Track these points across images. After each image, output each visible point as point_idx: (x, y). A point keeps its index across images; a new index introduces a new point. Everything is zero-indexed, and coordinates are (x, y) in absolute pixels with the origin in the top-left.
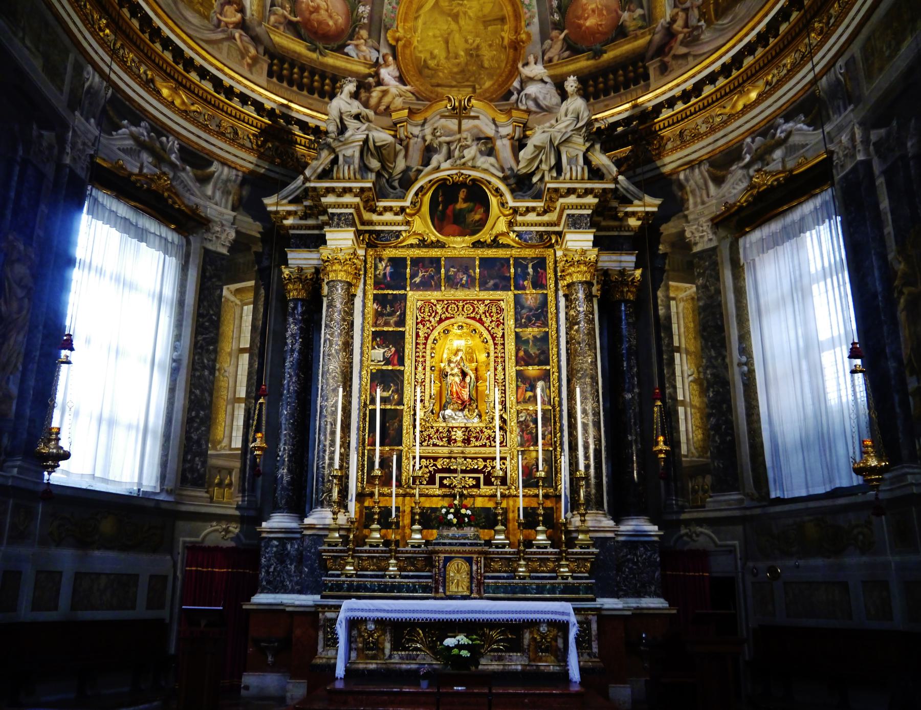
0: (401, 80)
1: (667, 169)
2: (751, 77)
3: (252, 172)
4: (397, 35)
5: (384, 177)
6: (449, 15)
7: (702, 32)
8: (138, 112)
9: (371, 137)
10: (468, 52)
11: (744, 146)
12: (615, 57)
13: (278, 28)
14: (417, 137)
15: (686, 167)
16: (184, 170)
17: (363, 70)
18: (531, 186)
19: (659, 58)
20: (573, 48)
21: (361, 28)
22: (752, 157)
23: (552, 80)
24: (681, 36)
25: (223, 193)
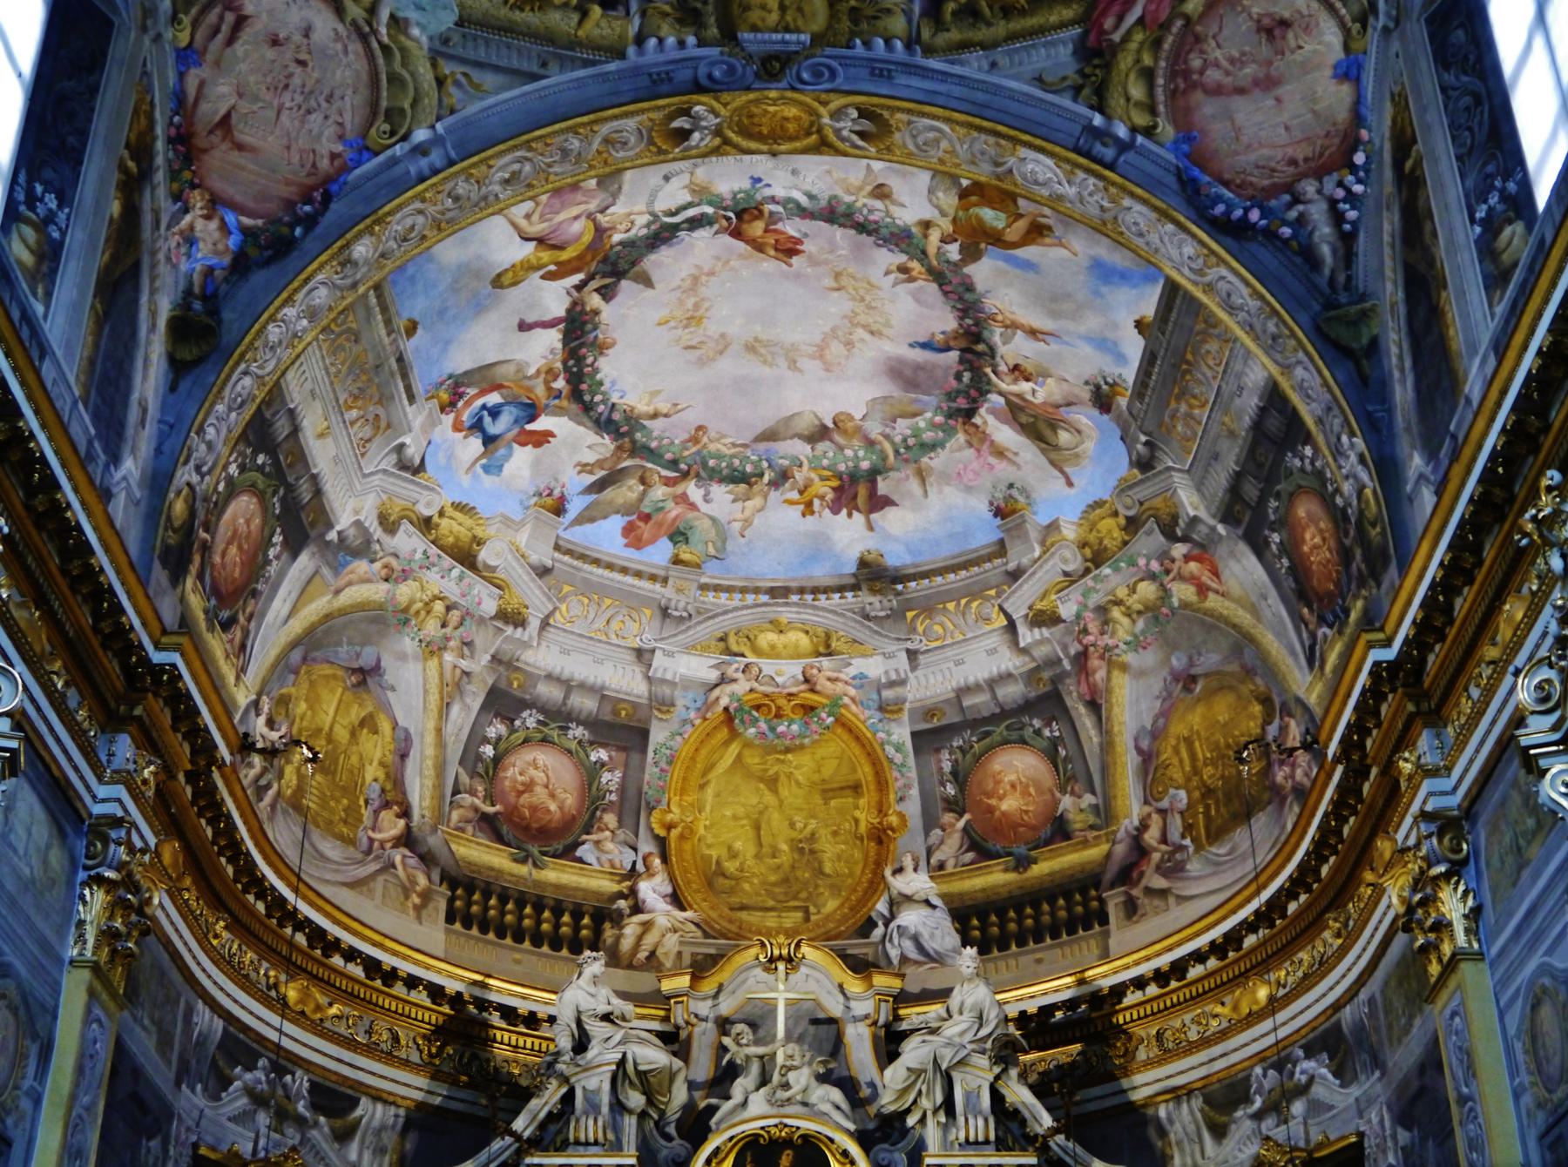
0: (677, 900)
1: (1137, 1096)
2: (1262, 965)
3: (421, 1105)
4: (669, 817)
6: (761, 780)
8: (255, 1045)
9: (630, 1057)
12: (1051, 874)
13: (462, 830)
14: (705, 1020)
15: (1167, 1097)
16: (316, 1124)
17: (608, 886)
18: (905, 1132)
20: (980, 848)
21: (604, 811)
23: (946, 904)
24: (1156, 856)
25: (374, 1152)
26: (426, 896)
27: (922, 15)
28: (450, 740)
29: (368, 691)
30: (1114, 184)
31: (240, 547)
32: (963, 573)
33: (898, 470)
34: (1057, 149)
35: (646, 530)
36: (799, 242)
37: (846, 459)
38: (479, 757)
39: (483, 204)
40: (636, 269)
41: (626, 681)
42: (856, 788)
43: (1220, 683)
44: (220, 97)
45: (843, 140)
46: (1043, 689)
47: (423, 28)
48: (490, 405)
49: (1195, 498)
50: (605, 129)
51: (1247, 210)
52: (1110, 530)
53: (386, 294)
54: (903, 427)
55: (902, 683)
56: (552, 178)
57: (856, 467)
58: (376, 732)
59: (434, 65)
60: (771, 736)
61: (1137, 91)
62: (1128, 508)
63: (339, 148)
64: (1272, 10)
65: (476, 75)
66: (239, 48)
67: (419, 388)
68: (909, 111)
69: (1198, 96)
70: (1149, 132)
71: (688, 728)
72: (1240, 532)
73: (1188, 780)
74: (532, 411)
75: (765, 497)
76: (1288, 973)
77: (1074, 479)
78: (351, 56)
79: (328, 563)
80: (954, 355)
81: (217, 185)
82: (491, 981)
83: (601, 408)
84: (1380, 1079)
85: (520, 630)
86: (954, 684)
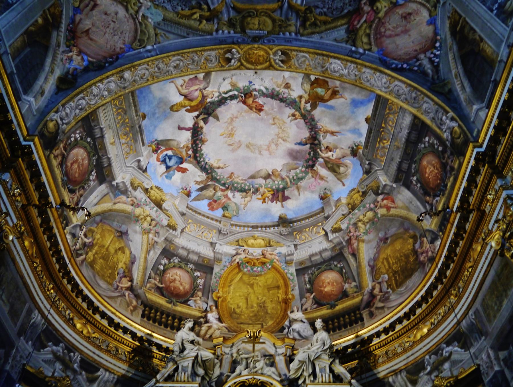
0: (220, 320)
1: (381, 375)
3: (124, 376)
4: (219, 295)
5: (206, 379)
6: (248, 284)
7: (390, 295)
8: (59, 337)
10: (259, 305)
11: (425, 360)
12: (343, 309)
13: (151, 290)
14: (228, 354)
15: (392, 374)
16: (81, 374)
17: (198, 314)
19: (368, 309)
20: (319, 303)
21: (198, 291)
22: (431, 368)
24: (379, 297)
26: (135, 308)
27: (300, 25)
28: (149, 262)
29: (122, 239)
30: (359, 64)
31: (78, 166)
32: (311, 219)
33: (291, 187)
34: (342, 56)
35: (215, 205)
36: (263, 106)
37: (276, 185)
38: (158, 269)
39: (167, 74)
40: (214, 113)
41: (207, 252)
42: (278, 287)
43: (396, 237)
44: (87, 24)
45: (276, 64)
46: (337, 252)
47: (152, 20)
48: (168, 155)
49: (385, 178)
50: (206, 54)
51: (402, 65)
52: (357, 197)
53: (136, 100)
54: (293, 173)
55: (293, 254)
56: (189, 69)
57: (278, 187)
58: (124, 253)
59: (155, 30)
60: (251, 271)
61: (365, 40)
62: (363, 189)
63: (123, 46)
64: (406, 11)
65: (167, 34)
66: (94, 12)
67: (146, 141)
68: (296, 51)
69: (384, 39)
70: (370, 50)
71: (226, 268)
72: (401, 183)
73: (388, 271)
74: (181, 161)
75: (251, 197)
76: (435, 320)
77: (345, 183)
78: (129, 23)
79: (112, 192)
80: (308, 146)
81: (82, 48)
82: (154, 334)
83: (203, 163)
84: (485, 340)
85: (174, 231)
86: (309, 254)
